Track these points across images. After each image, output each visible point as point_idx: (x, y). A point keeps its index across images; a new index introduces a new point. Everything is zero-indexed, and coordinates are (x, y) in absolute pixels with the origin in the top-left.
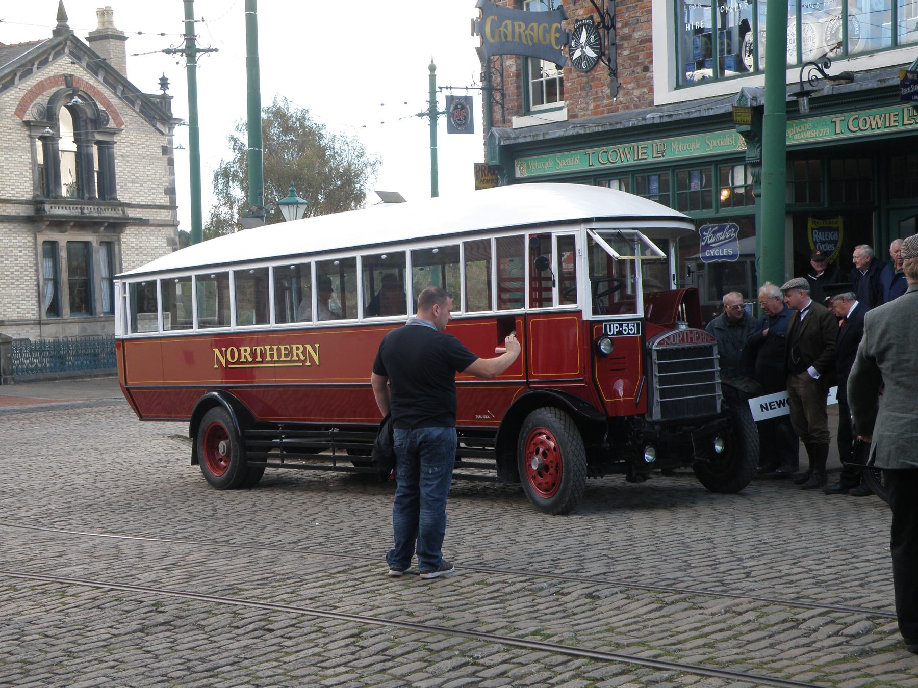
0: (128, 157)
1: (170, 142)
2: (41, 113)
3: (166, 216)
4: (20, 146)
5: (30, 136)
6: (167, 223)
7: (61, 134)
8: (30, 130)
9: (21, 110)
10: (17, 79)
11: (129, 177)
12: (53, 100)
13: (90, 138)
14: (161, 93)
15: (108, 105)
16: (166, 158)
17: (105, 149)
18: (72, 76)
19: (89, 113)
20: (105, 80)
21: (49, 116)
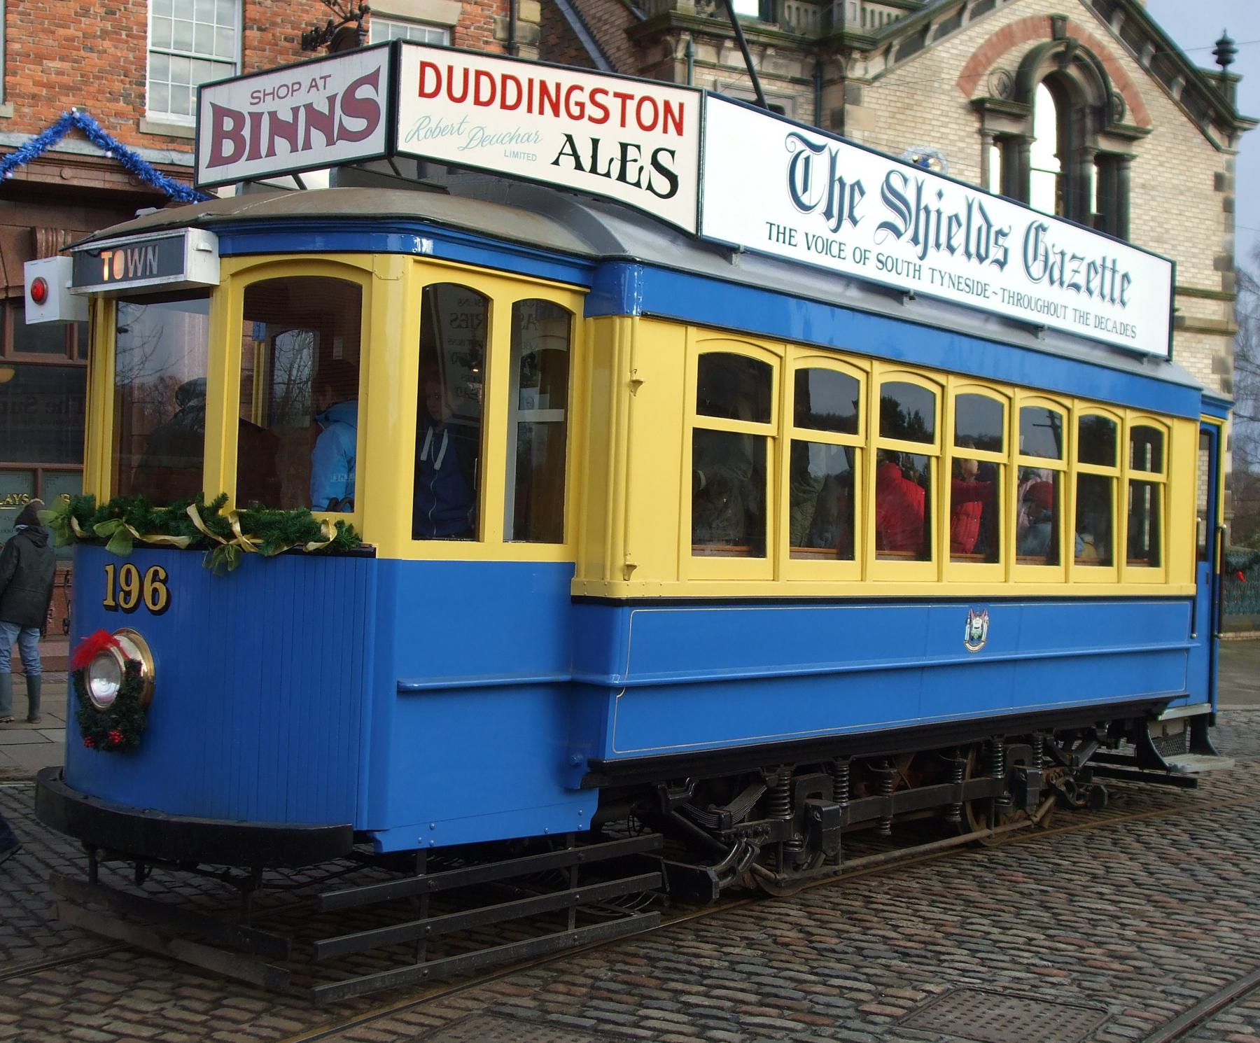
0: (1153, 188)
1: (1230, 167)
2: (1004, 88)
3: (1214, 313)
4: (961, 150)
5: (982, 133)
6: (1215, 326)
7: (1036, 135)
8: (982, 121)
9: (970, 75)
10: (966, 15)
11: (1152, 230)
12: (1029, 61)
13: (1089, 144)
14: (1218, 68)
15: (1125, 86)
16: (1219, 197)
17: (1113, 166)
18: (1064, 19)
19: (1090, 95)
20: (1123, 31)
21: (1018, 96)
